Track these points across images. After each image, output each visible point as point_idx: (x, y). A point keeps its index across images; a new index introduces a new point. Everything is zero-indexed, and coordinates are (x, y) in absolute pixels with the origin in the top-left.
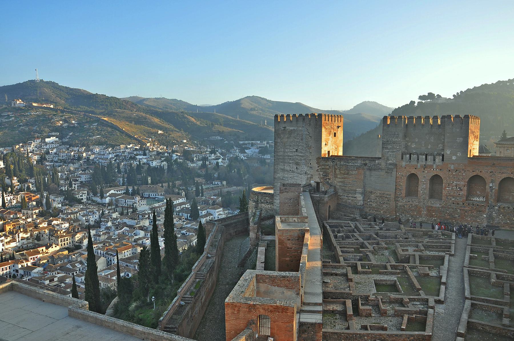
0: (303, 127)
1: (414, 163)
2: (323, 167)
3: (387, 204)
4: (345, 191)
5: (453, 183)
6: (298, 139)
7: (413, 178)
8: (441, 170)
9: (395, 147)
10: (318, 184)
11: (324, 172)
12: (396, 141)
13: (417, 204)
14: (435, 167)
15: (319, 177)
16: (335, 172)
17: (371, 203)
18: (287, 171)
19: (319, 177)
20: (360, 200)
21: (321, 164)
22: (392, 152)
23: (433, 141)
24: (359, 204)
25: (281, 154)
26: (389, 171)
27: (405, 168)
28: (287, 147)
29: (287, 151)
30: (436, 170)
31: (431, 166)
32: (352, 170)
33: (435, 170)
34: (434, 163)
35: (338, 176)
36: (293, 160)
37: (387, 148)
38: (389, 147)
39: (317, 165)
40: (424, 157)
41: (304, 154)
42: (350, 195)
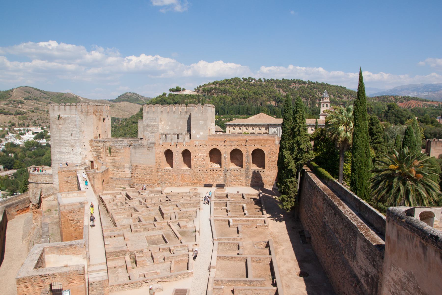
0: (76, 114)
1: (169, 141)
2: (95, 148)
3: (150, 175)
4: (115, 166)
5: (198, 155)
7: (169, 154)
10: (92, 162)
11: (97, 152)
13: (173, 173)
14: (184, 144)
15: (92, 157)
17: (137, 175)
18: (64, 153)
19: (92, 157)
20: (128, 173)
21: (94, 145)
23: (182, 124)
24: (128, 177)
26: (150, 149)
28: (62, 132)
29: (62, 135)
31: (182, 143)
32: (120, 149)
37: (147, 130)
38: (149, 129)
39: (90, 147)
40: (176, 136)
42: (120, 170)
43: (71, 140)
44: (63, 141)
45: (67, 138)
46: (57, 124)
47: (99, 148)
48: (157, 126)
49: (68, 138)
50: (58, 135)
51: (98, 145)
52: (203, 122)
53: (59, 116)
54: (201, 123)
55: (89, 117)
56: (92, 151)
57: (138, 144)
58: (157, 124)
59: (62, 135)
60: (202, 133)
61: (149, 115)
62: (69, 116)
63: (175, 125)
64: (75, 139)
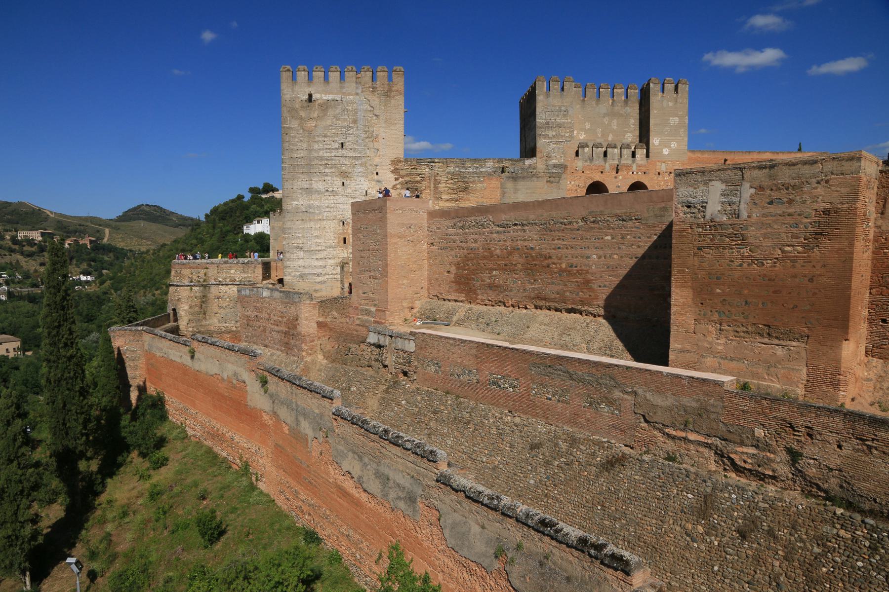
0: (357, 94)
2: (408, 179)
6: (345, 120)
8: (645, 173)
9: (563, 134)
12: (564, 122)
14: (634, 168)
16: (436, 187)
18: (318, 192)
21: (403, 172)
22: (556, 143)
23: (615, 127)
25: (301, 154)
26: (552, 179)
27: (583, 172)
28: (317, 139)
29: (316, 147)
30: (637, 173)
31: (628, 167)
32: (473, 182)
33: (635, 173)
34: (634, 162)
35: (444, 196)
36: (334, 166)
37: (546, 136)
38: (551, 133)
39: (392, 176)
41: (360, 153)
43: (342, 159)
44: (317, 162)
45: (328, 154)
46: (301, 118)
47: (418, 178)
48: (570, 128)
49: (333, 154)
50: (305, 146)
51: (415, 171)
52: (676, 119)
53: (310, 96)
54: (672, 123)
55: (393, 101)
56: (398, 186)
57: (522, 169)
58: (570, 122)
59: (316, 147)
60: (674, 145)
61: (550, 99)
62: (338, 97)
63: (599, 130)
64: (351, 157)
